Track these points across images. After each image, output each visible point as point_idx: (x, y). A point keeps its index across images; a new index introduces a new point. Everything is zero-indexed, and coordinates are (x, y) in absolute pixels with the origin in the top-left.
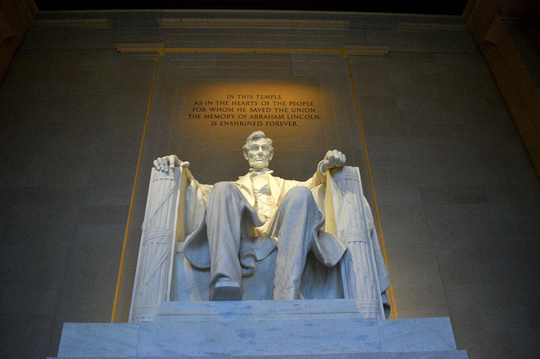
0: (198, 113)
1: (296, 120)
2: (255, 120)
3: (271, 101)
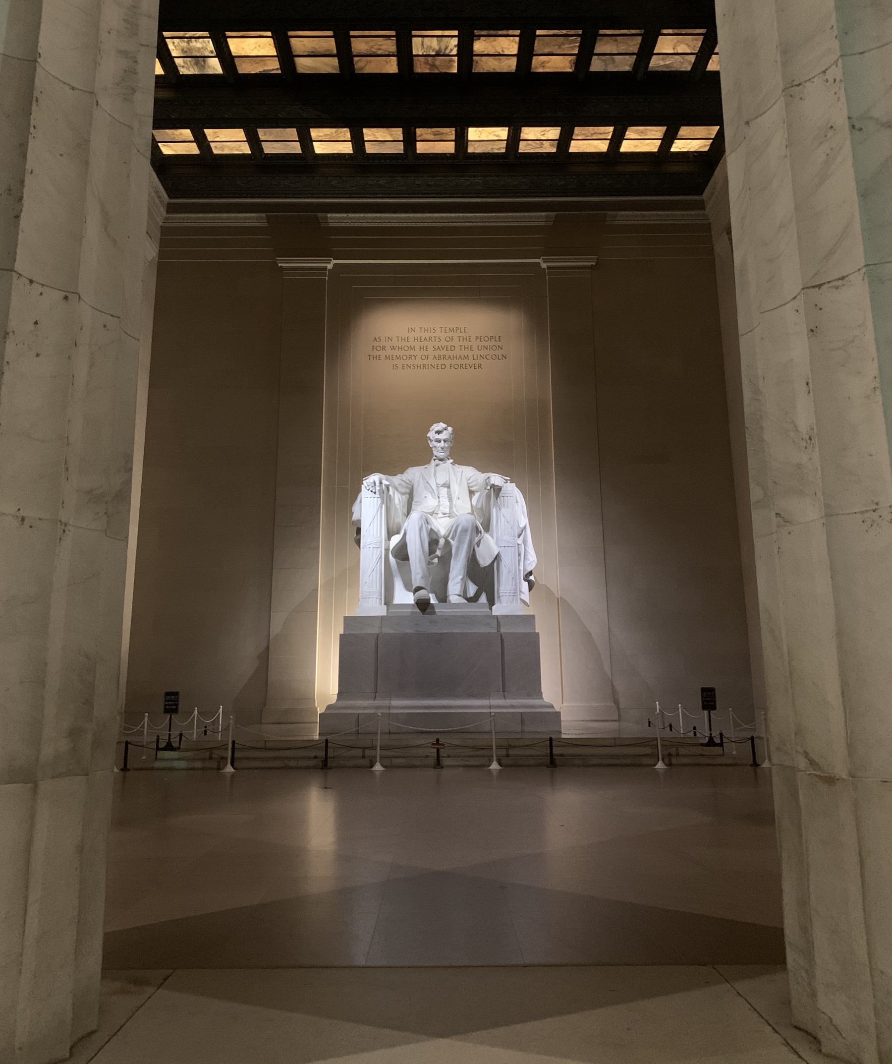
0: (377, 353)
1: (482, 361)
2: (437, 362)
3: (455, 335)
